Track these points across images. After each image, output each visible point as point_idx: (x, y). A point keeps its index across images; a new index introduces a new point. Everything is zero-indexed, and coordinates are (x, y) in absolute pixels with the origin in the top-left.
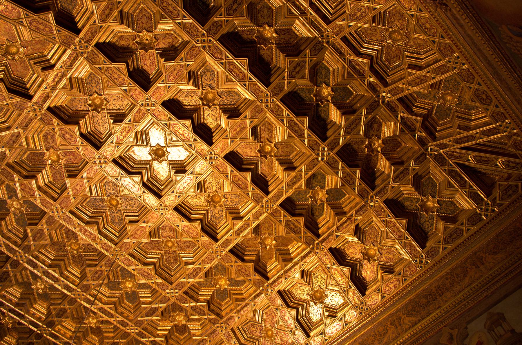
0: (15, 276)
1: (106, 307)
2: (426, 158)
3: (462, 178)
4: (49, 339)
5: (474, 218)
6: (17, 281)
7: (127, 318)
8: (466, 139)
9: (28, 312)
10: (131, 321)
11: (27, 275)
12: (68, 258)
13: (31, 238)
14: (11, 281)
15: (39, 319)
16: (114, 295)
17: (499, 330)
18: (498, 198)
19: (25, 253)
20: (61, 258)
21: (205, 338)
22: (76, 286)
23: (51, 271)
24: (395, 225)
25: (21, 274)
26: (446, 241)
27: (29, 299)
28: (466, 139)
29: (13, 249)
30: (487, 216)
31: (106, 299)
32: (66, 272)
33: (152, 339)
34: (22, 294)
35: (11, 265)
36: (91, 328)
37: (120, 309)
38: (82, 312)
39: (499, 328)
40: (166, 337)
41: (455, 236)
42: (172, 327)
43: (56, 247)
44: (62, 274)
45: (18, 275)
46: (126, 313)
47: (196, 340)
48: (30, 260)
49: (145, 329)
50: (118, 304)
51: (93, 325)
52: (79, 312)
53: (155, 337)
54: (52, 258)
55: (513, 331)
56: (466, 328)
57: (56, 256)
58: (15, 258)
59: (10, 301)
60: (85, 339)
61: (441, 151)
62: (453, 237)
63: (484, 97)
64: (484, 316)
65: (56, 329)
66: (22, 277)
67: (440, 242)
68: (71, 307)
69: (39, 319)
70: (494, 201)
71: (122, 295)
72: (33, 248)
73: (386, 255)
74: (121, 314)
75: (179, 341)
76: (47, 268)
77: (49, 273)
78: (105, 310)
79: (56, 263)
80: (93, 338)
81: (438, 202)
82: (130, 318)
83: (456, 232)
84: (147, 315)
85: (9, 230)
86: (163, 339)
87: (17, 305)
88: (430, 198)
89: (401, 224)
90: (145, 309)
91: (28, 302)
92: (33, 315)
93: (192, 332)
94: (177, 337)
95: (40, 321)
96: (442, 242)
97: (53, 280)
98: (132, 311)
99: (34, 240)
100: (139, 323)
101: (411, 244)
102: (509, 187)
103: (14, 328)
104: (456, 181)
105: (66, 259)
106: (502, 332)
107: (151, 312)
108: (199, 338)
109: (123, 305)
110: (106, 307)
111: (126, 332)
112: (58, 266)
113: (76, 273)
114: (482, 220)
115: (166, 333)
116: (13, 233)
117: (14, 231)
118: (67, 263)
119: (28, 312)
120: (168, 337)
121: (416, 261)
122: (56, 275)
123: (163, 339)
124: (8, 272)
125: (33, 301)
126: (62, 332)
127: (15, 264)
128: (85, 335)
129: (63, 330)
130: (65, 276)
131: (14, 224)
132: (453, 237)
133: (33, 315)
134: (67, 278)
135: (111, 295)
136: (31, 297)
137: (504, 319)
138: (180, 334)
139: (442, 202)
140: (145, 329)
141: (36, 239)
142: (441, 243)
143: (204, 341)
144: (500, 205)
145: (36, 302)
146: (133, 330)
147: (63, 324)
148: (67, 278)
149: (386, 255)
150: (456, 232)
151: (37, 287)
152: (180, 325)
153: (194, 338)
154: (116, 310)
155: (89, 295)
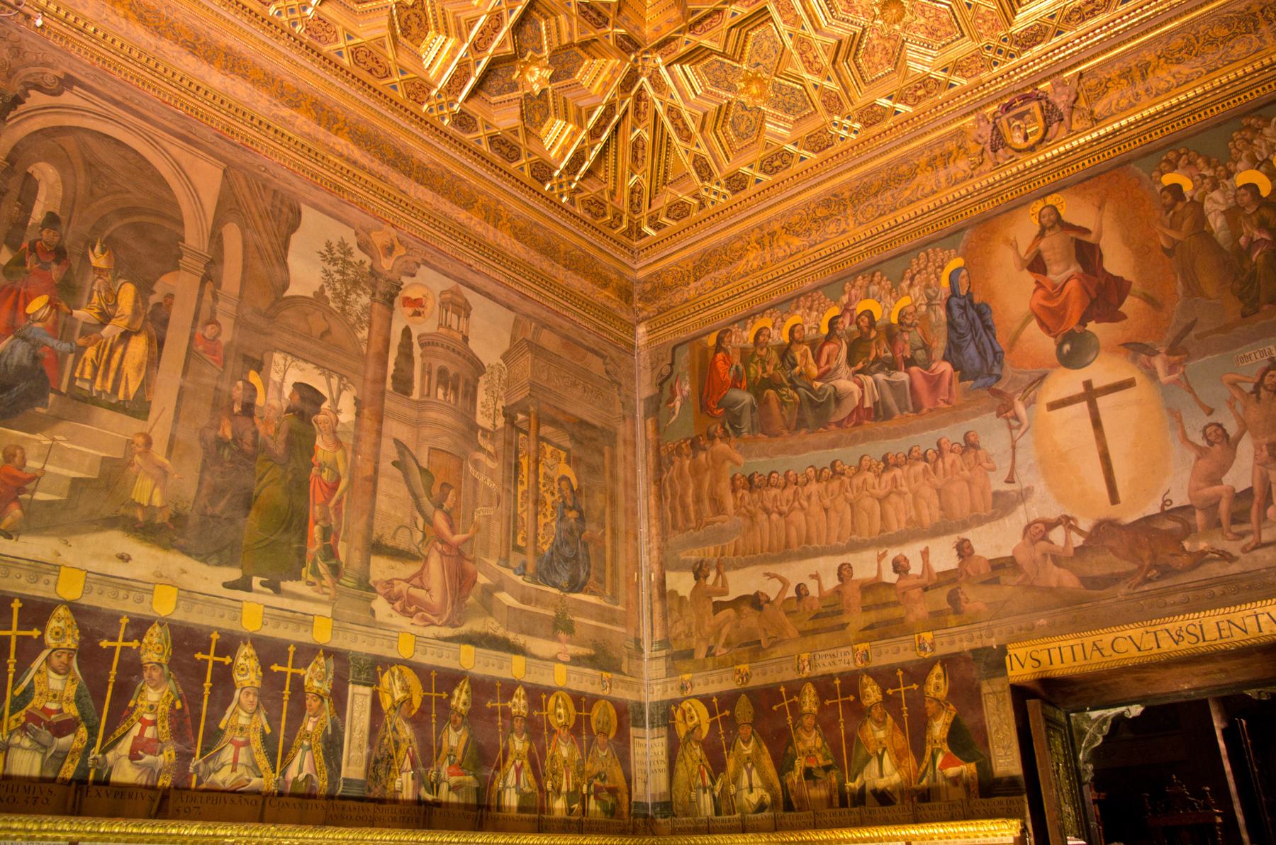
2: (629, 53)
3: (605, 127)
5: (542, 171)
8: (681, 126)
17: (453, 319)
18: (581, 195)
24: (496, 30)
26: (492, 139)
28: (681, 126)
30: (552, 189)
39: (455, 317)
41: (506, 150)
55: (466, 339)
56: (418, 265)
61: (644, 79)
62: (503, 148)
63: (776, 164)
64: (450, 284)
67: (350, 38)
70: (578, 190)
73: (412, 17)
81: (544, 91)
83: (511, 150)
88: (547, 73)
89: (503, 43)
96: (405, 77)
101: (468, 75)
102: (602, 204)
104: (599, 121)
106: (454, 326)
114: (543, 183)
121: (439, 96)
132: (503, 148)
137: (468, 316)
139: (543, 97)
142: (487, 132)
144: (572, 201)
149: (412, 17)
150: (511, 150)
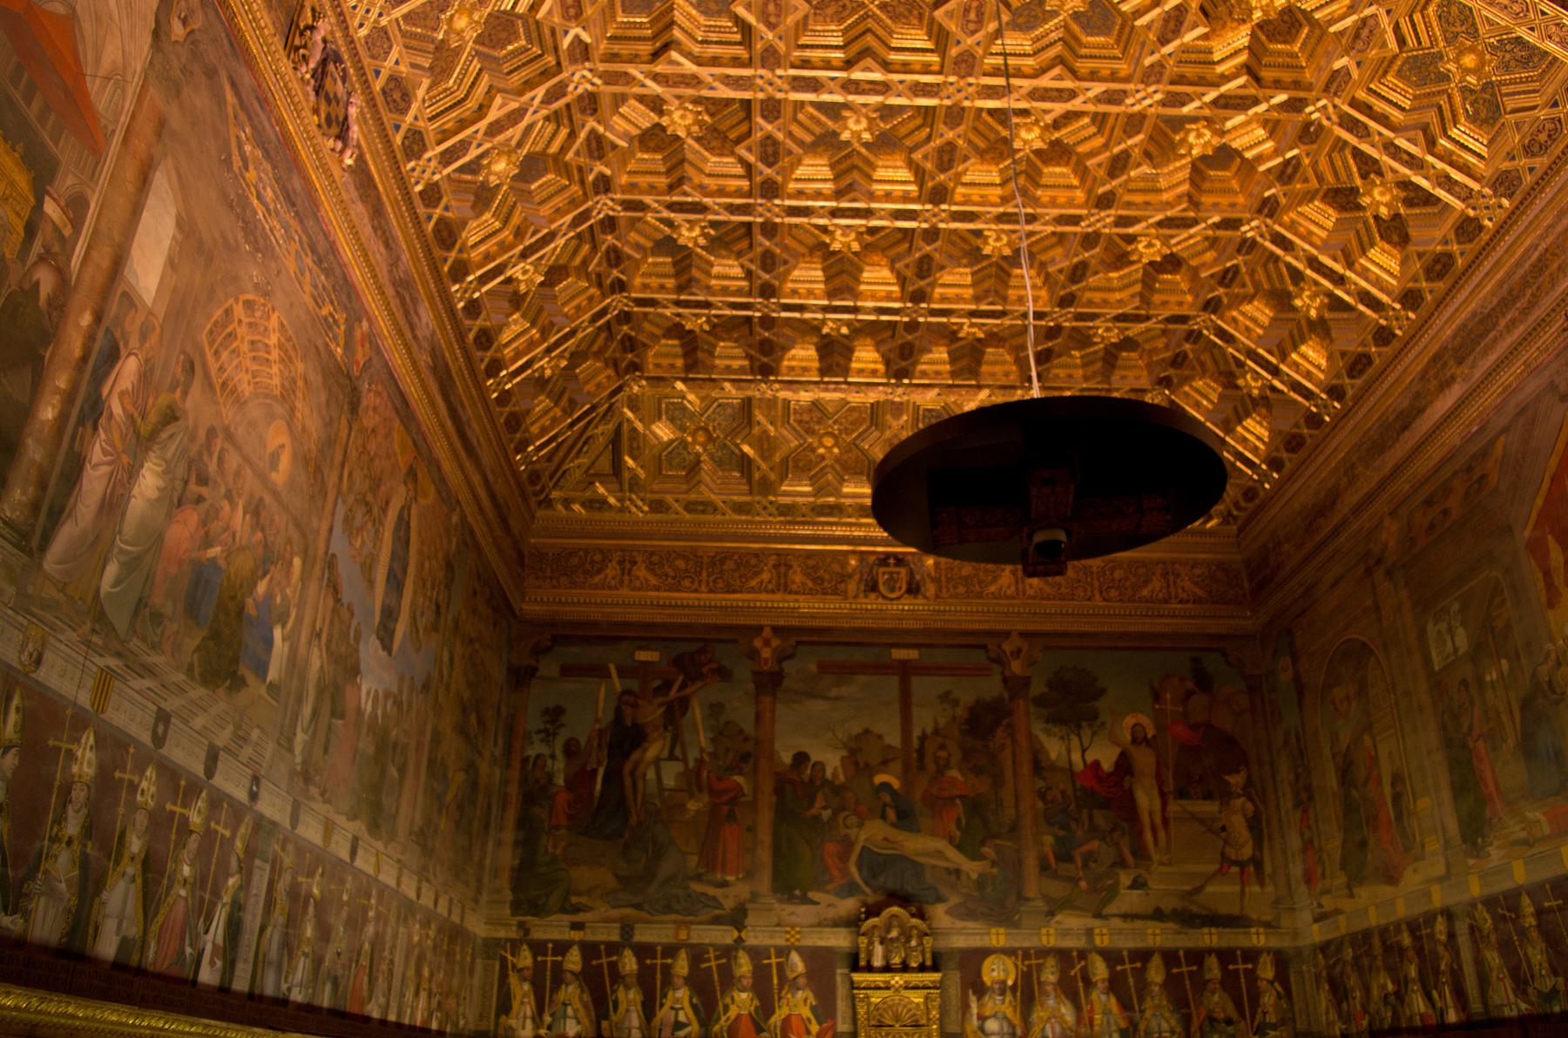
0: (790, 134)
1: (1045, 82)
4: (955, 230)
6: (800, 143)
7: (1113, 77)
9: (872, 197)
10: (1127, 80)
11: (812, 117)
12: (874, 17)
13: (762, 27)
14: (790, 153)
15: (906, 198)
16: (1046, 41)
19: (773, 70)
20: (861, 28)
21: (1367, 12)
22: (940, 73)
23: (857, 75)
25: (800, 124)
27: (854, 167)
29: (741, 78)
31: (1030, 62)
32: (893, 57)
33: (1212, 95)
34: (832, 166)
35: (764, 117)
36: (1038, 152)
37: (1083, 66)
38: (991, 128)
40: (1248, 69)
42: (1253, 35)
43: (830, 11)
44: (887, 66)
45: (795, 129)
46: (1105, 67)
47: (1342, 33)
48: (795, 78)
49: (1179, 80)
50: (1068, 57)
51: (1039, 145)
52: (987, 132)
53: (1217, 86)
54: (839, 41)
57: (845, 32)
58: (761, 96)
59: (818, 195)
60: (1038, 185)
65: (958, 198)
66: (807, 129)
68: (961, 129)
69: (906, 198)
71: (1066, 27)
72: (781, 47)
74: (1093, 76)
75: (1294, 62)
76: (843, 75)
77: (857, 83)
78: (1046, 90)
79: (855, 48)
80: (1056, 172)
82: (1122, 74)
84: (1164, 41)
85: (702, 42)
86: (1242, 80)
87: (839, 194)
90: (1148, 27)
91: (856, 175)
92: (888, 196)
93: (1317, 16)
94: (1279, 53)
95: (913, 201)
97: (877, 93)
98: (1117, 53)
99: (771, 26)
100: (1153, 74)
103: (867, 247)
105: (870, 23)
107: (1172, 25)
108: (1349, 21)
109: (1084, 51)
110: (1045, 82)
111: (1131, 116)
112: (866, 52)
113: (919, 45)
115: (1243, 58)
116: (716, 43)
117: (714, 37)
118: (880, 32)
119: (872, 197)
120: (1255, 66)
122: (877, 76)
123: (1242, 80)
124: (769, 137)
125: (866, 168)
126: (976, 198)
127: (772, 109)
128: (1033, 176)
129: (975, 193)
130: (897, 67)
131: (702, 19)
133: (888, 196)
134: (906, 68)
135: (1039, 45)
136: (856, 161)
138: (1285, 42)
140: (1179, 80)
141: (773, 20)
143: (1371, 22)
145: (873, 167)
146: (1146, 100)
147: (966, 179)
148: (906, 68)
151: (853, 133)
152: (1273, 16)
153: (1332, 29)
154: (1075, 75)
155: (985, 75)
